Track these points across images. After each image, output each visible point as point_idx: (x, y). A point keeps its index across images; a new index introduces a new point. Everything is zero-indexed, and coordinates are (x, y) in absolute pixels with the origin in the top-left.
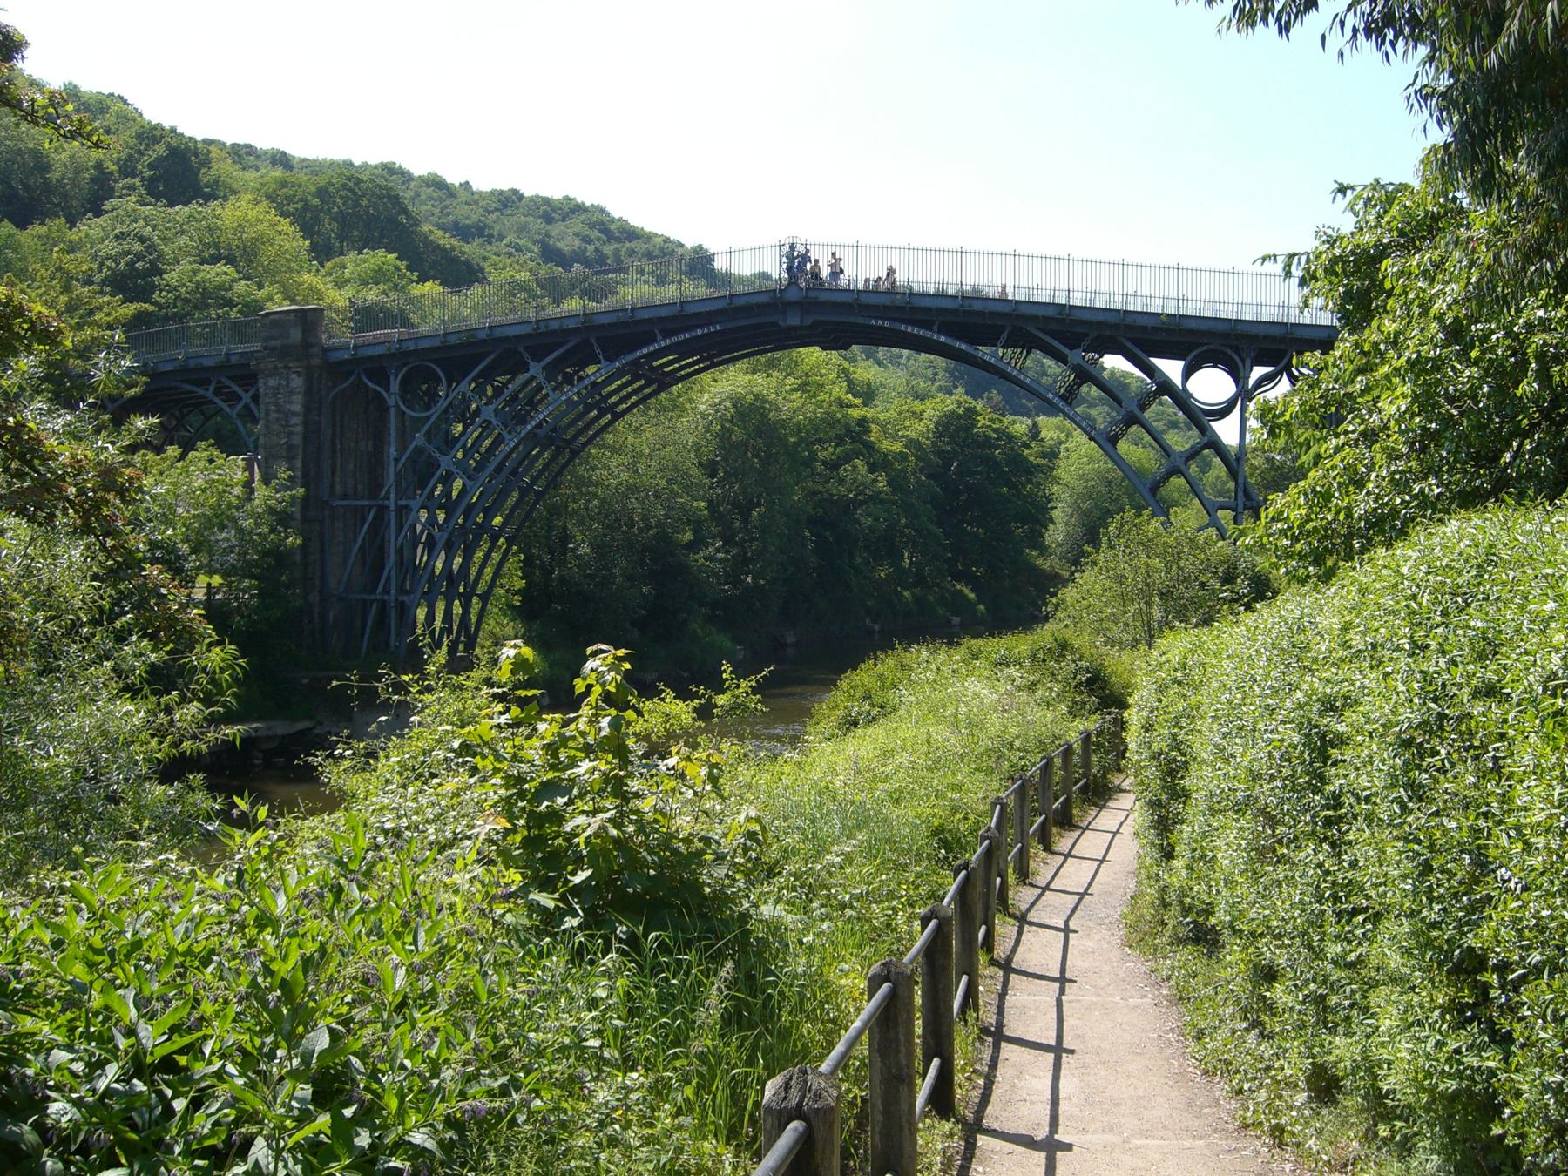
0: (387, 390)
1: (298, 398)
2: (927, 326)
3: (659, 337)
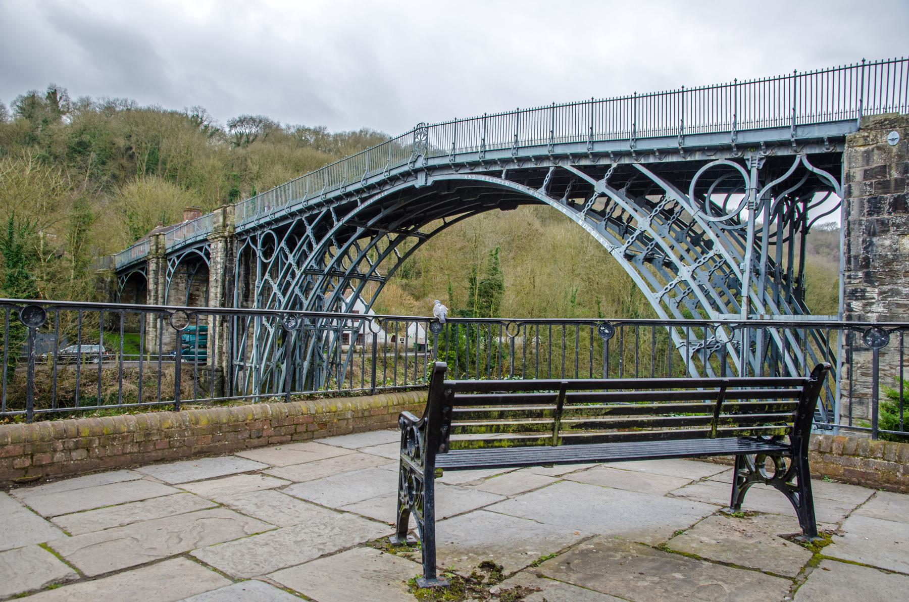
0: (257, 247)
1: (219, 254)
2: (498, 174)
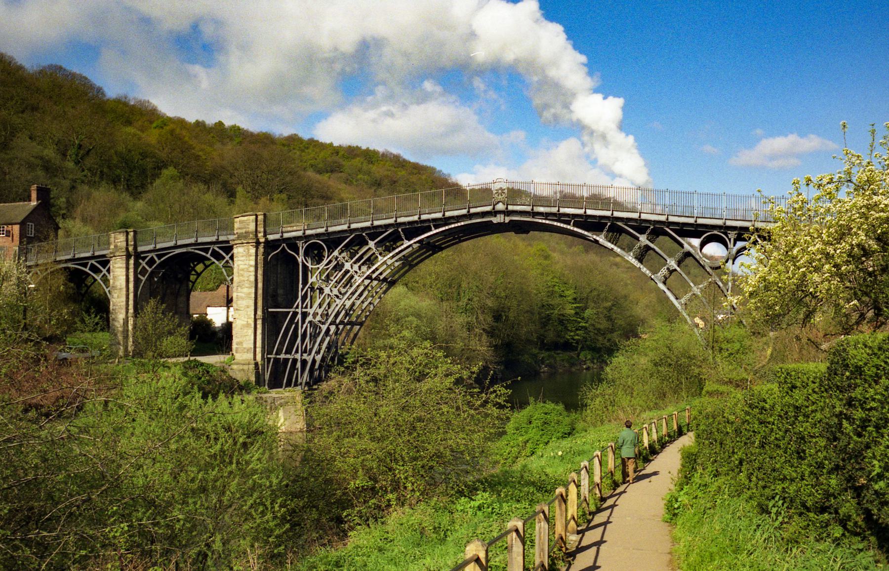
2: (568, 223)
3: (433, 228)
